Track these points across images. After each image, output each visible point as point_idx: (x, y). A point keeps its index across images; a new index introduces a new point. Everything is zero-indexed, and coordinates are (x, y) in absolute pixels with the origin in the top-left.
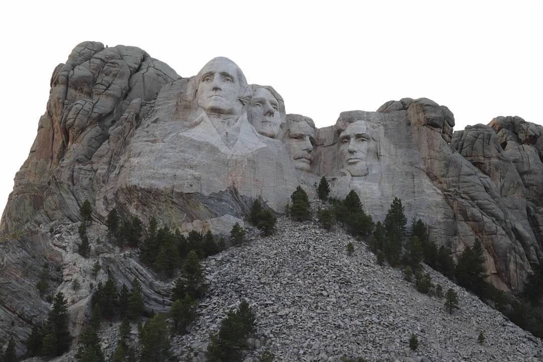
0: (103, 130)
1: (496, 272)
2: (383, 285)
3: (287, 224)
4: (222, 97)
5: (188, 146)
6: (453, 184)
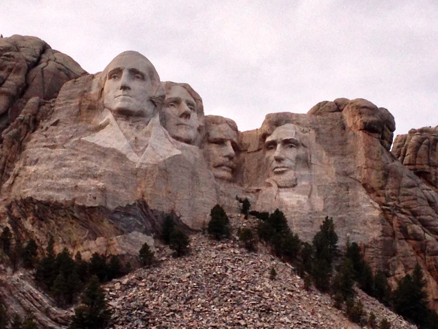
2: (309, 313)
3: (203, 243)
4: (131, 96)
5: (91, 152)
6: (393, 197)
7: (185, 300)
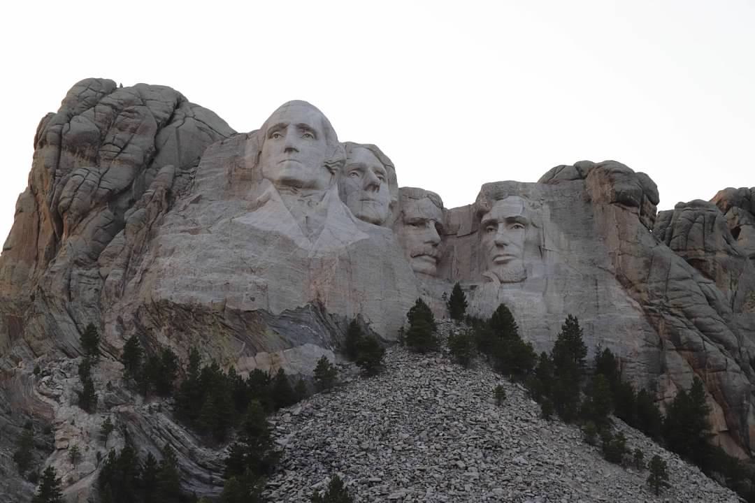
0: (115, 214)
1: (726, 429)
2: (552, 451)
3: (401, 358)
4: (298, 161)
5: (247, 238)
6: (658, 294)
7: (380, 436)
